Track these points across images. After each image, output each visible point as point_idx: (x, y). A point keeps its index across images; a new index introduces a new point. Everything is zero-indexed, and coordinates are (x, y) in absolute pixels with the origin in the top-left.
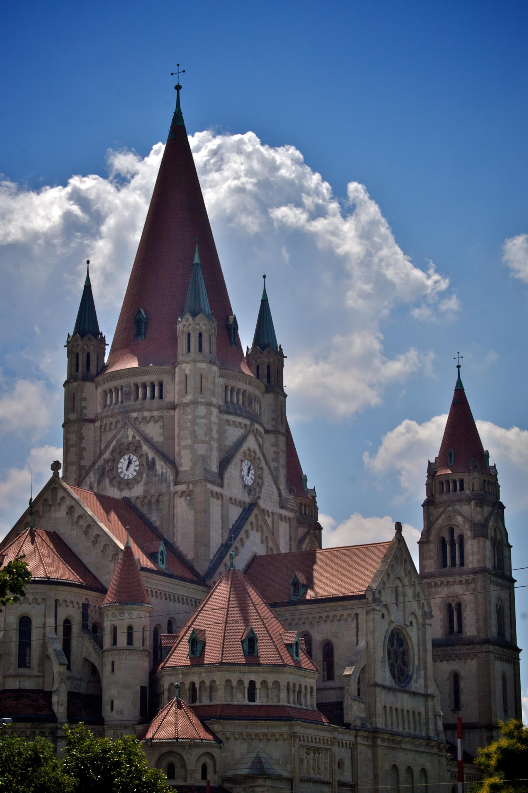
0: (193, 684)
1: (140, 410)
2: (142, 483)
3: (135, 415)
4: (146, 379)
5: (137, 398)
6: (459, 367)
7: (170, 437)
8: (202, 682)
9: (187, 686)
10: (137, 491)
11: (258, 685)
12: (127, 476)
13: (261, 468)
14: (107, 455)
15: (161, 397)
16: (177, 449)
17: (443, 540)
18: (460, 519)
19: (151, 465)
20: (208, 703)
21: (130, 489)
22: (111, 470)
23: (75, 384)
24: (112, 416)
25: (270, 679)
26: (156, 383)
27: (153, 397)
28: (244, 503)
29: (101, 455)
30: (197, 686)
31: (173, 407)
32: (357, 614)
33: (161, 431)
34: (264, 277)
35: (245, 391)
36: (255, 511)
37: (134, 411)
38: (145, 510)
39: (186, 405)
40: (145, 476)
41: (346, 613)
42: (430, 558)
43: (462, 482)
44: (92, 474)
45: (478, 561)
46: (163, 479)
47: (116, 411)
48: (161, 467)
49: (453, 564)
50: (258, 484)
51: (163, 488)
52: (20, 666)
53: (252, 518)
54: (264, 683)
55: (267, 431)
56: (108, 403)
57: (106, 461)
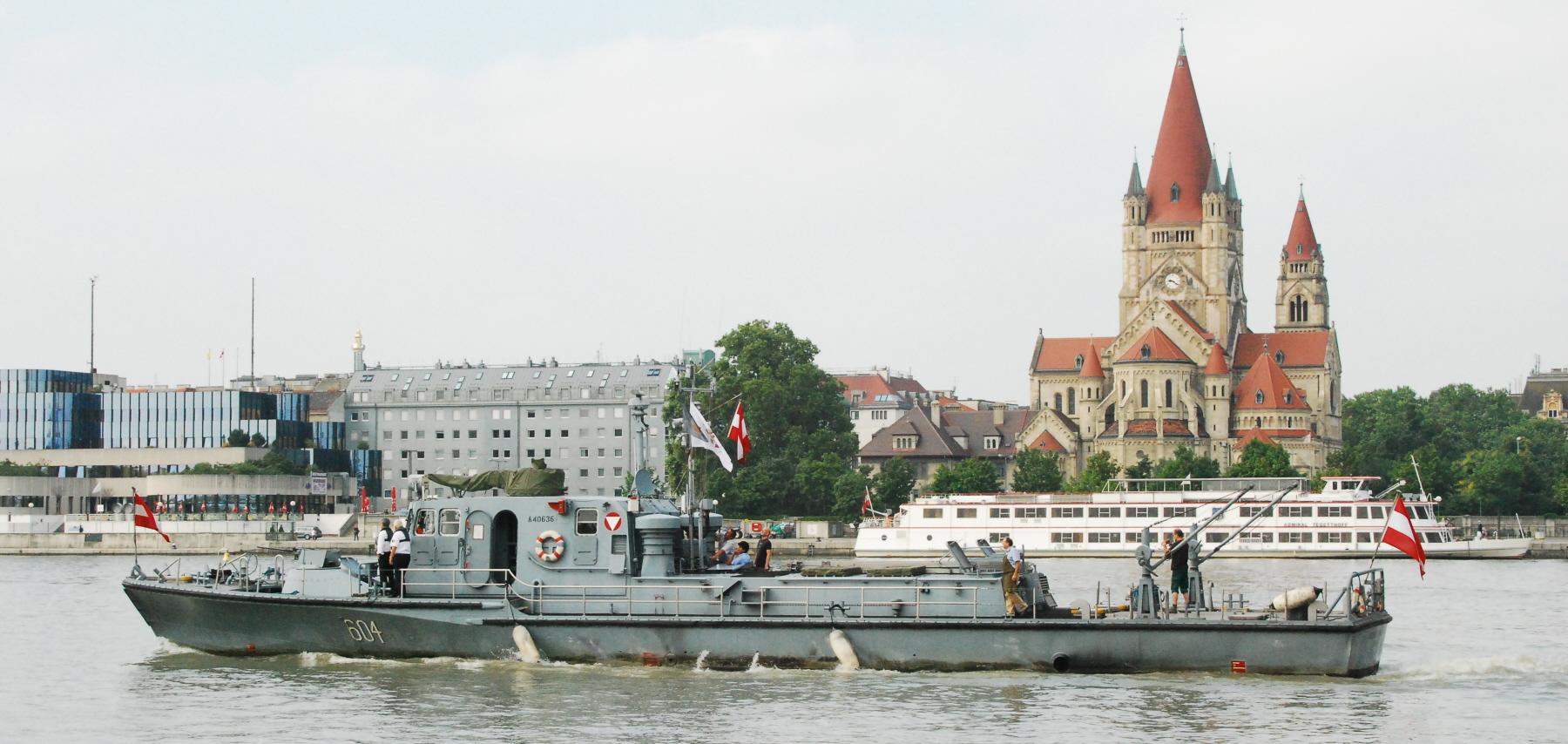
0: (1259, 418)
1: (1182, 248)
2: (1184, 292)
3: (1178, 251)
4: (1184, 229)
5: (1177, 240)
6: (1301, 185)
7: (1200, 266)
8: (1265, 418)
9: (1256, 418)
10: (1180, 297)
11: (1293, 419)
14: (1159, 273)
15: (1192, 240)
16: (1205, 273)
17: (1292, 304)
18: (1305, 291)
19: (1190, 283)
20: (1268, 428)
21: (1175, 295)
22: (1161, 283)
23: (1133, 227)
24: (1161, 250)
25: (1298, 415)
29: (1154, 273)
30: (1262, 419)
31: (1201, 248)
37: (1177, 248)
38: (1186, 309)
39: (1212, 248)
40: (1185, 288)
41: (1311, 374)
42: (1284, 315)
43: (1306, 265)
44: (1148, 284)
45: (1318, 319)
46: (1198, 291)
47: (1165, 247)
48: (1196, 283)
49: (1299, 319)
51: (1198, 297)
52: (1167, 406)
54: (1296, 418)
57: (1160, 277)
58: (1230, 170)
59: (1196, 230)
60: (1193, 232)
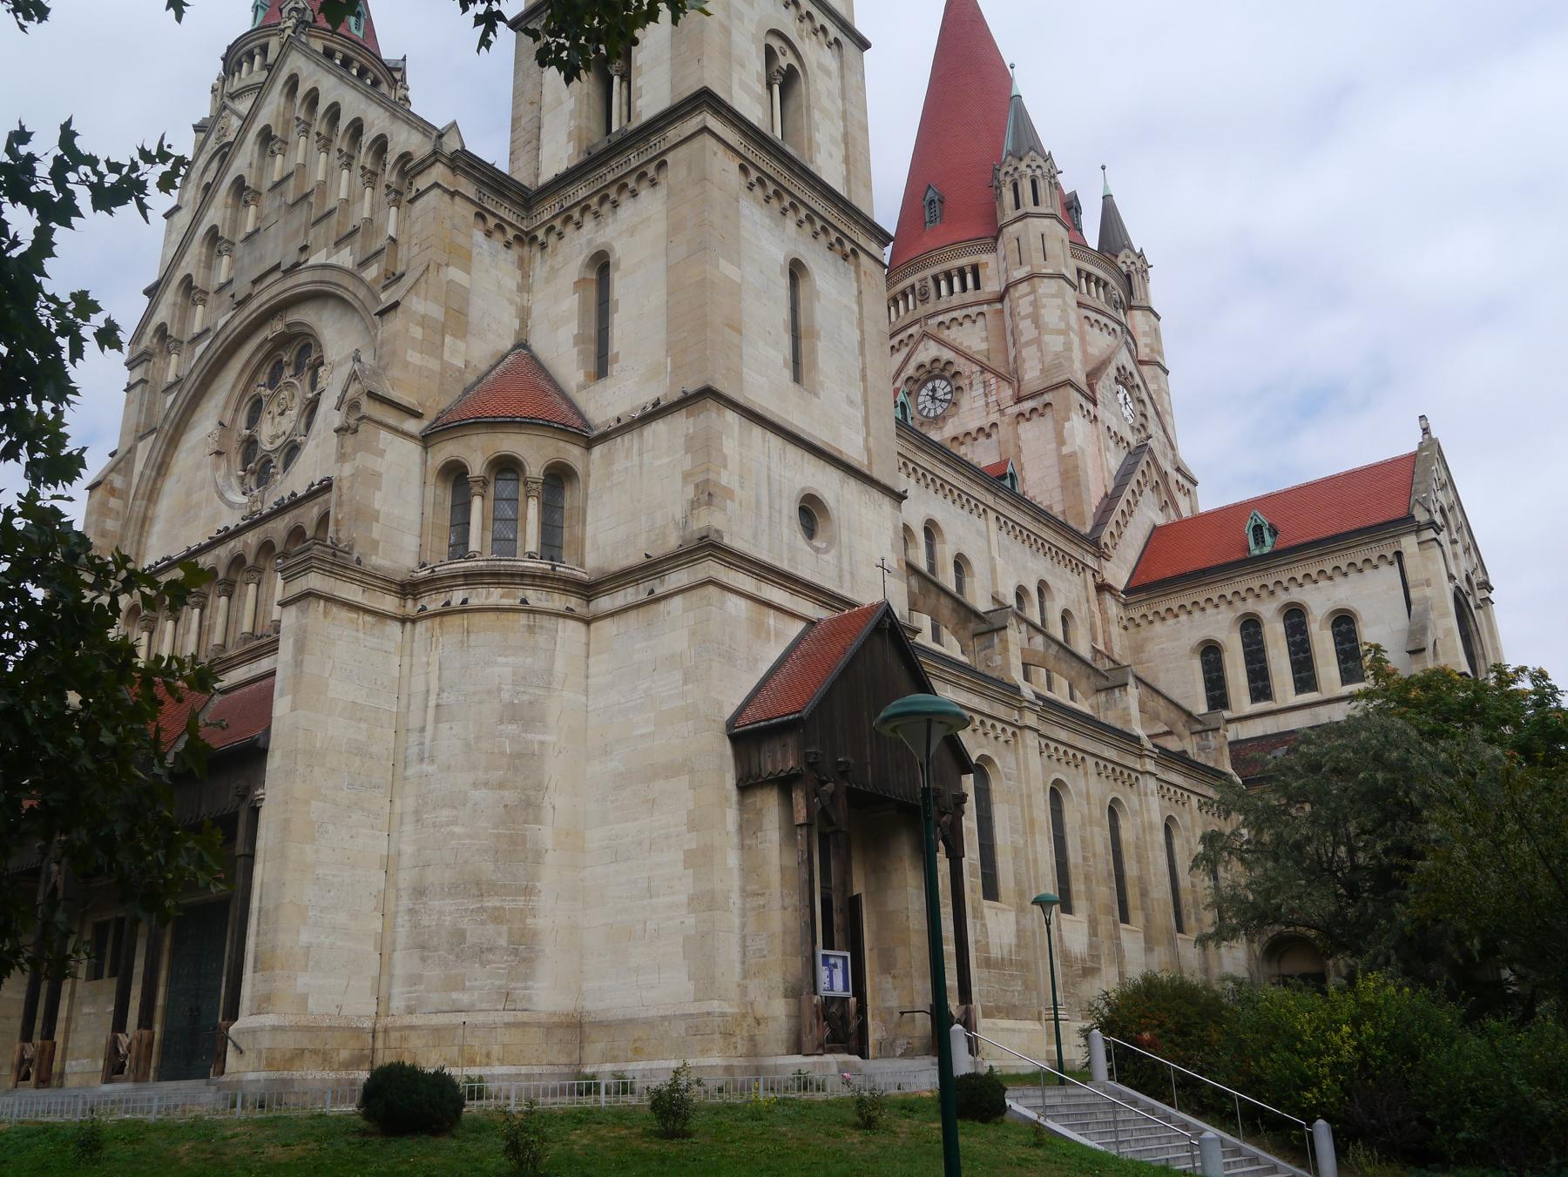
5: (939, 295)
12: (932, 411)
13: (1142, 402)
15: (977, 286)
26: (968, 269)
27: (964, 288)
28: (1128, 443)
32: (1399, 554)
33: (984, 334)
34: (1103, 168)
35: (1106, 284)
36: (1146, 457)
50: (1142, 425)
53: (1142, 466)
55: (1142, 362)
56: (893, 318)
58: (1108, 200)
59: (984, 258)
60: (975, 269)
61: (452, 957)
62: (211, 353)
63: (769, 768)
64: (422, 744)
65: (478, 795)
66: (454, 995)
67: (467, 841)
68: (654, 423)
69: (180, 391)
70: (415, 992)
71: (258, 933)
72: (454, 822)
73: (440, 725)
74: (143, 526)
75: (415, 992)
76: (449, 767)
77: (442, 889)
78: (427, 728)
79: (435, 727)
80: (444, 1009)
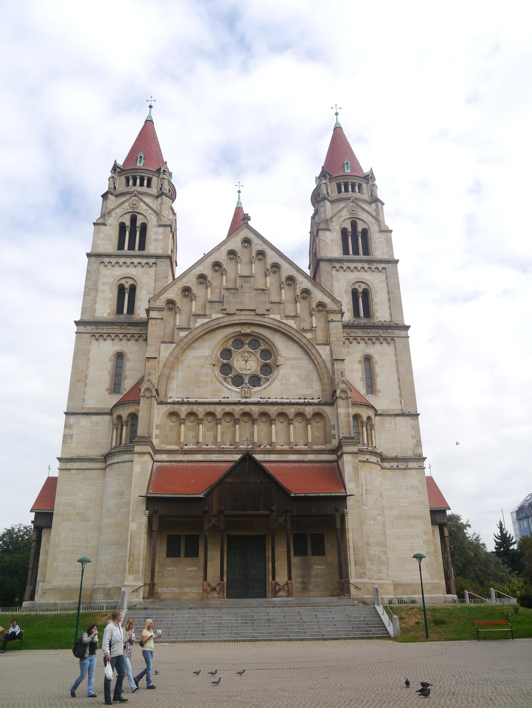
61: (379, 564)
62: (208, 325)
63: (439, 521)
64: (363, 500)
65: (379, 517)
66: (381, 575)
67: (378, 531)
68: (399, 417)
69: (190, 333)
70: (371, 573)
71: (354, 554)
72: (375, 525)
73: (368, 495)
74: (168, 379)
75: (371, 573)
76: (371, 508)
77: (374, 544)
78: (364, 495)
79: (366, 496)
80: (379, 579)
